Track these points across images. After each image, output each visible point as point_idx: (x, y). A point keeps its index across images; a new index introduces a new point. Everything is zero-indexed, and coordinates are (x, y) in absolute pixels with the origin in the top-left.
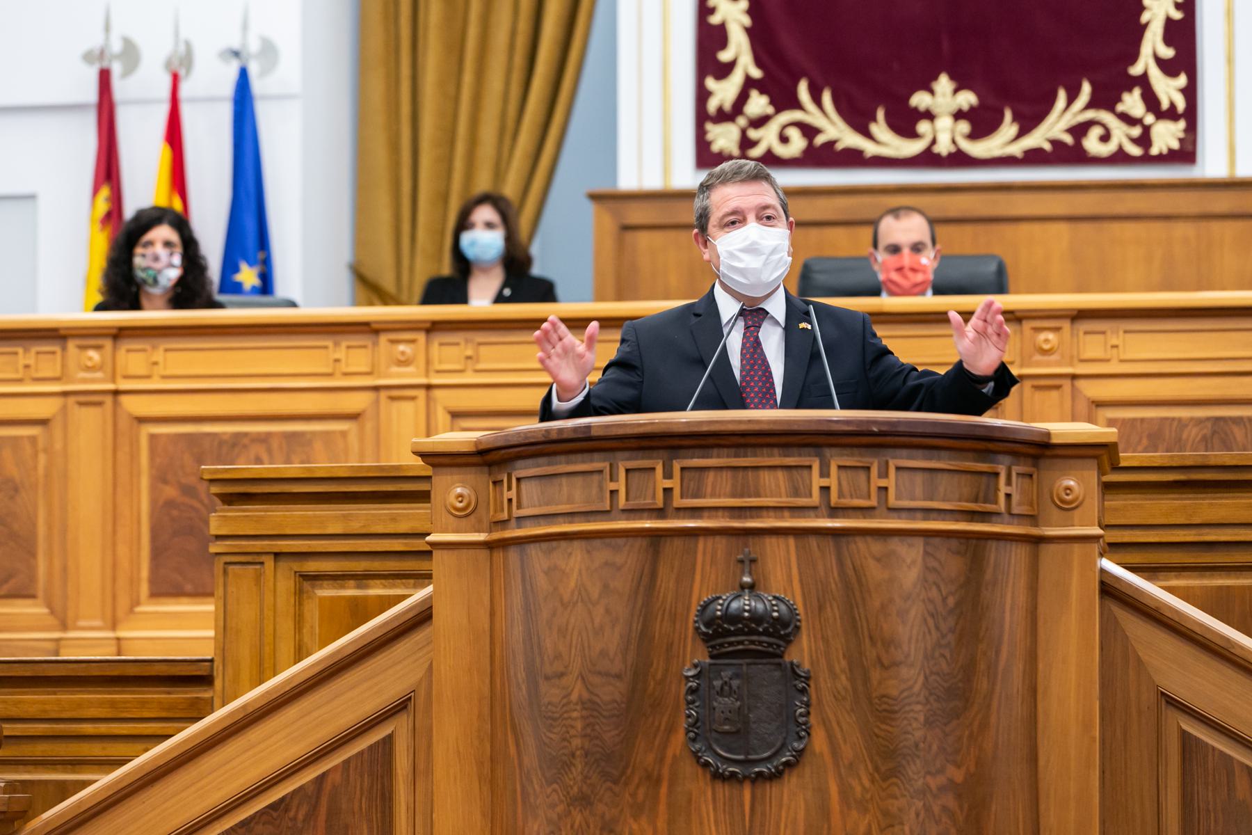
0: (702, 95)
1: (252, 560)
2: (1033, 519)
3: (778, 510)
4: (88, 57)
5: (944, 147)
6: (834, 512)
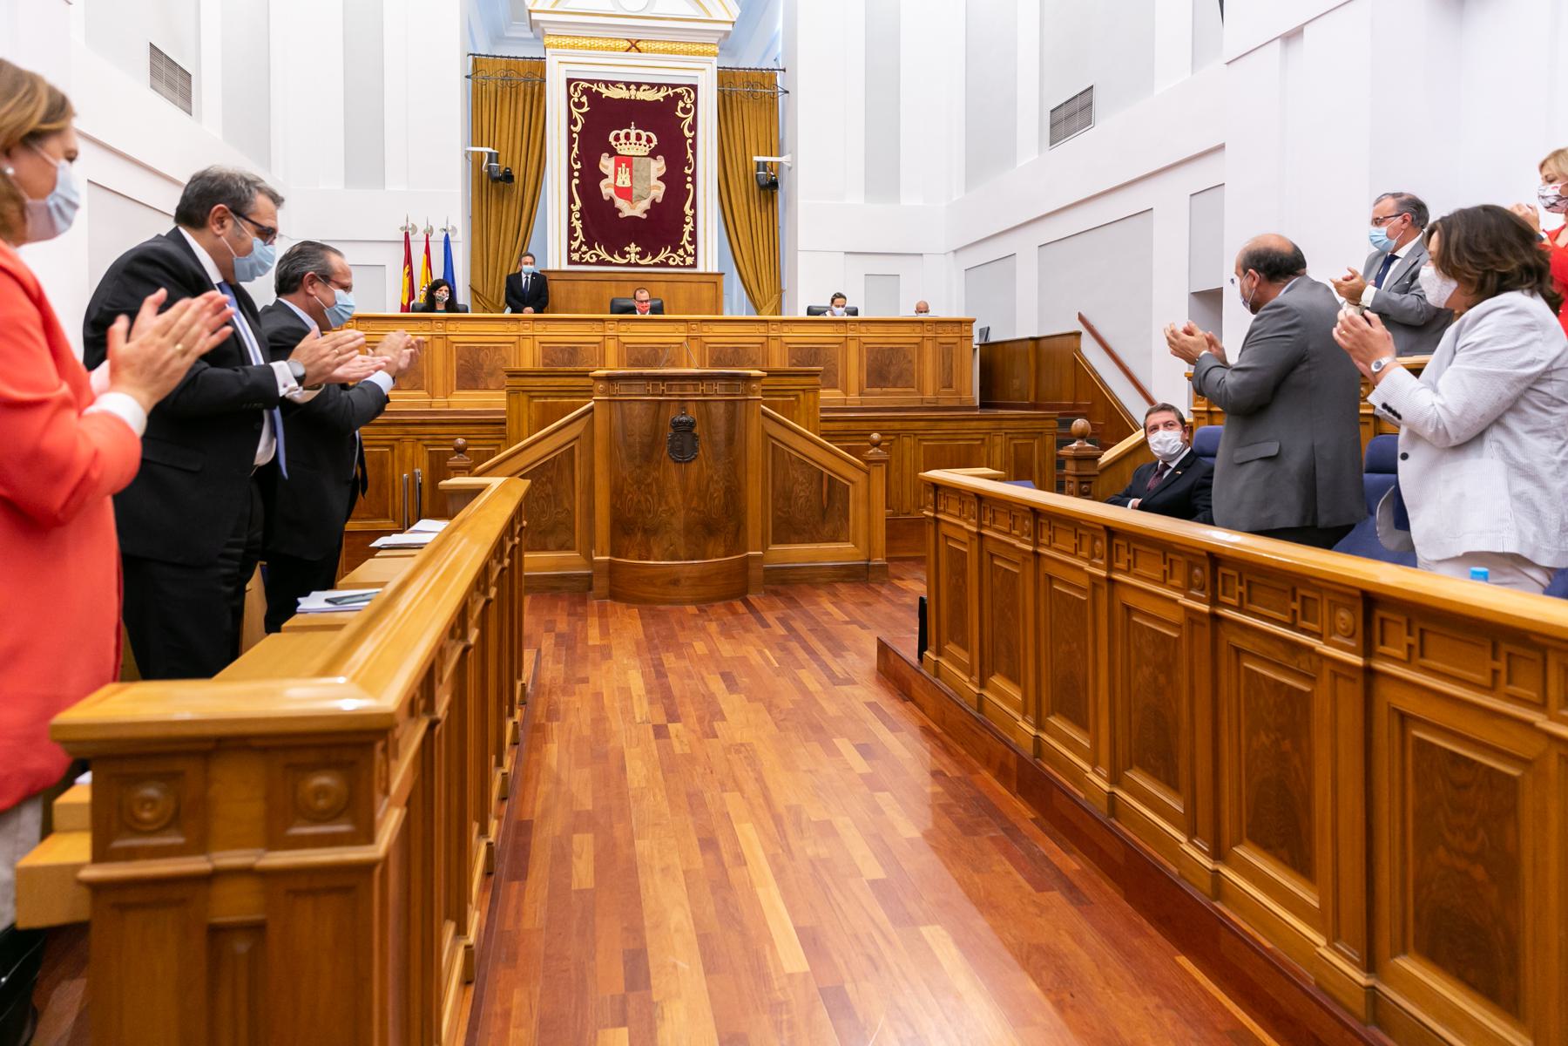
0: (570, 245)
1: (516, 392)
2: (745, 395)
3: (691, 395)
4: (402, 229)
5: (633, 261)
6: (705, 395)
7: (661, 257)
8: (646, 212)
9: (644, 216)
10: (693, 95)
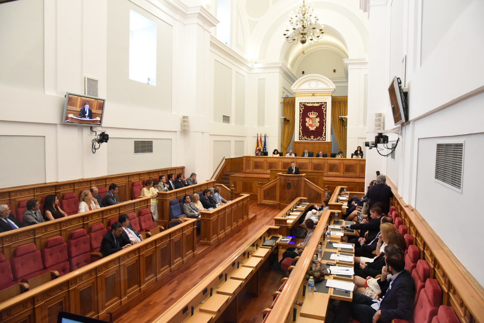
0: (299, 136)
7: (318, 138)
8: (315, 129)
9: (315, 130)
10: (326, 104)
